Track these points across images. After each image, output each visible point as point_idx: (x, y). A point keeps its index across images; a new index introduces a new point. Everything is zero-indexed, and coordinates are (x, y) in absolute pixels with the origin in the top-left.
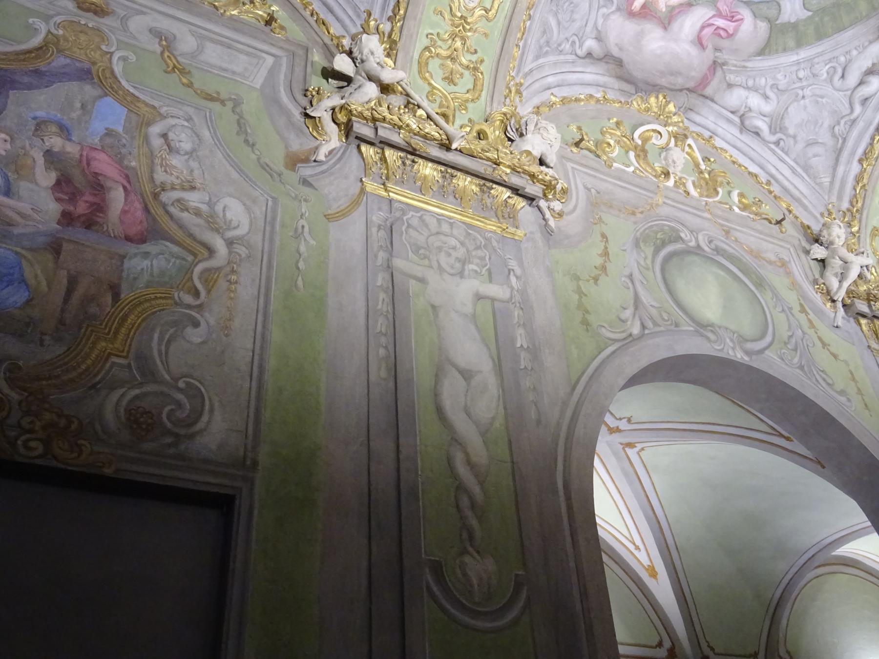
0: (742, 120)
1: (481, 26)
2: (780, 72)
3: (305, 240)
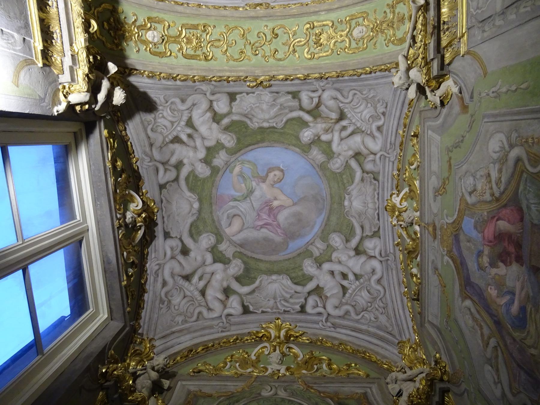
1: (372, 17)
3: (499, 89)
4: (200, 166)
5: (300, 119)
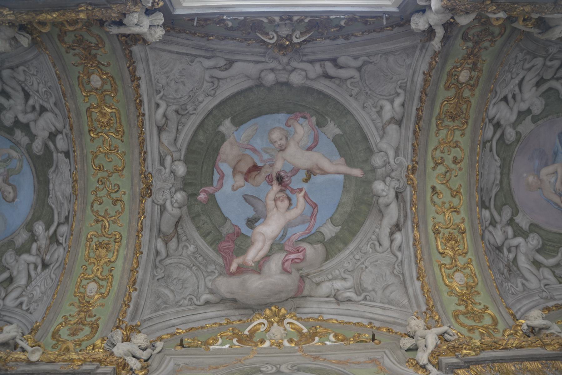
0: (336, 298)
2: (344, 262)
4: (11, 116)
5: (52, 222)
